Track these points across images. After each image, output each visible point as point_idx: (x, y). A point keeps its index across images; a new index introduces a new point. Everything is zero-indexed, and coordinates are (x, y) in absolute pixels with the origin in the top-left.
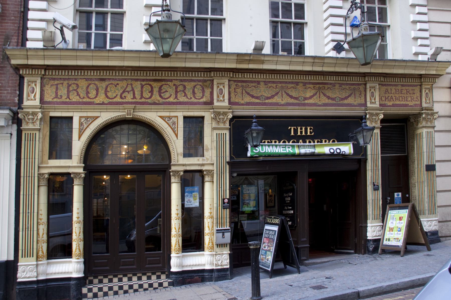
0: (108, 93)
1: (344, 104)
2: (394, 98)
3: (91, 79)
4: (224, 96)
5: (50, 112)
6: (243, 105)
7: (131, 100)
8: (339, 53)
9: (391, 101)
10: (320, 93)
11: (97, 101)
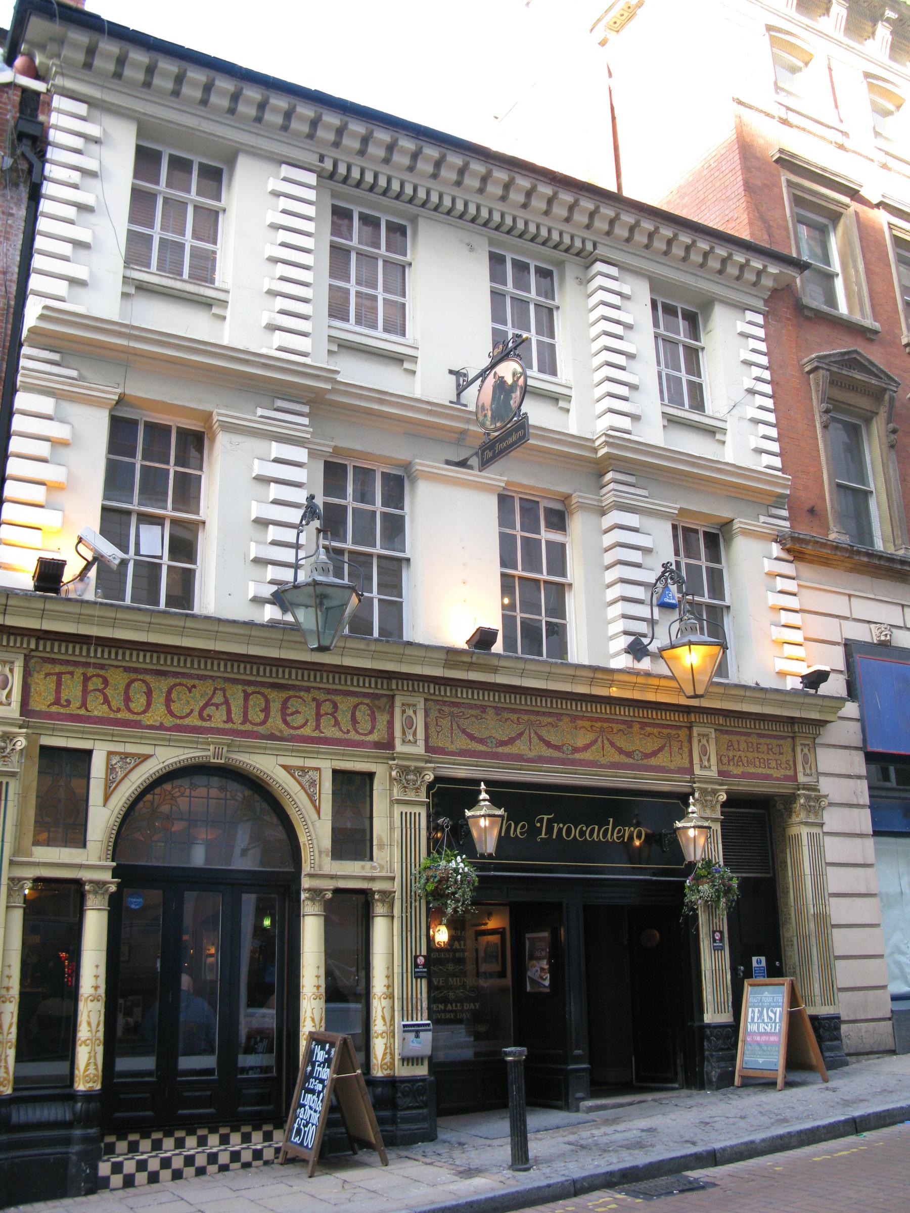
0: (172, 704)
1: (652, 766)
3: (135, 670)
4: (415, 734)
5: (42, 737)
6: (452, 753)
7: (221, 725)
8: (639, 661)
11: (147, 719)
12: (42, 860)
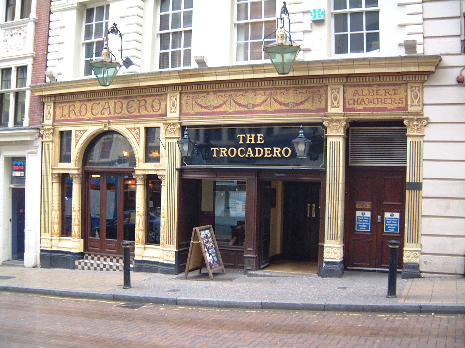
6: (192, 115)
7: (108, 116)
9: (362, 104)
10: (271, 100)
11: (86, 117)
12: (59, 168)
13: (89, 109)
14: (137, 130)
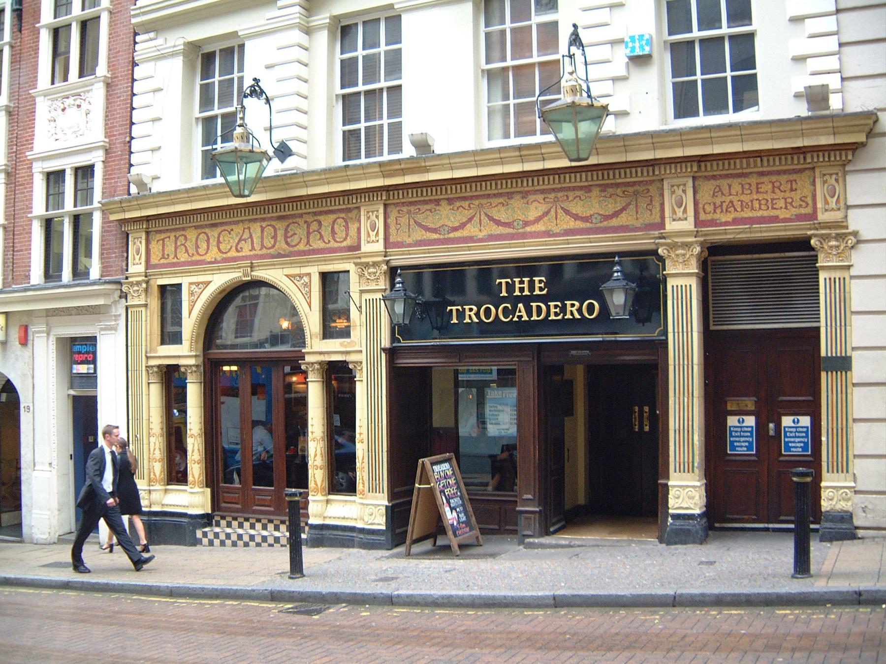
2: (738, 205)
6: (410, 245)
7: (249, 253)
9: (730, 212)
10: (556, 211)
11: (208, 258)
13: (213, 242)
14: (306, 279)
